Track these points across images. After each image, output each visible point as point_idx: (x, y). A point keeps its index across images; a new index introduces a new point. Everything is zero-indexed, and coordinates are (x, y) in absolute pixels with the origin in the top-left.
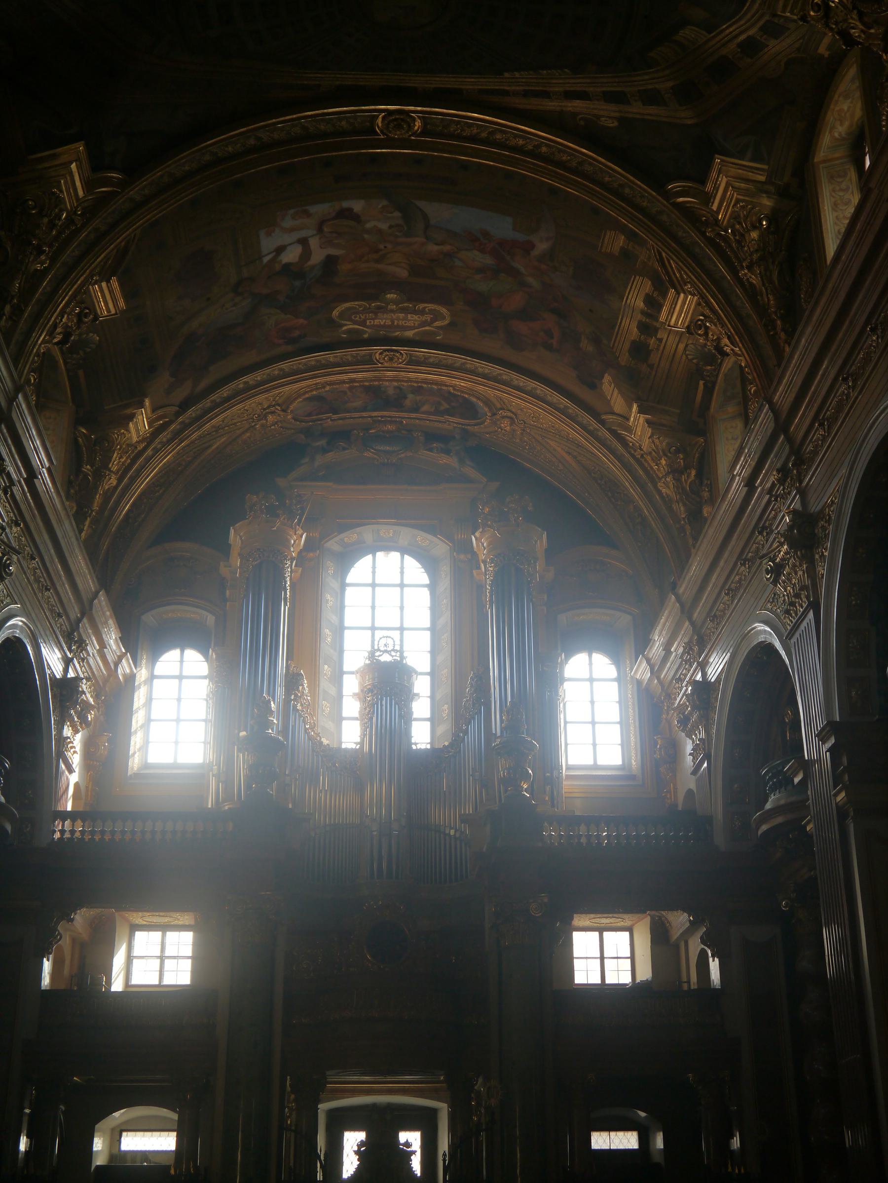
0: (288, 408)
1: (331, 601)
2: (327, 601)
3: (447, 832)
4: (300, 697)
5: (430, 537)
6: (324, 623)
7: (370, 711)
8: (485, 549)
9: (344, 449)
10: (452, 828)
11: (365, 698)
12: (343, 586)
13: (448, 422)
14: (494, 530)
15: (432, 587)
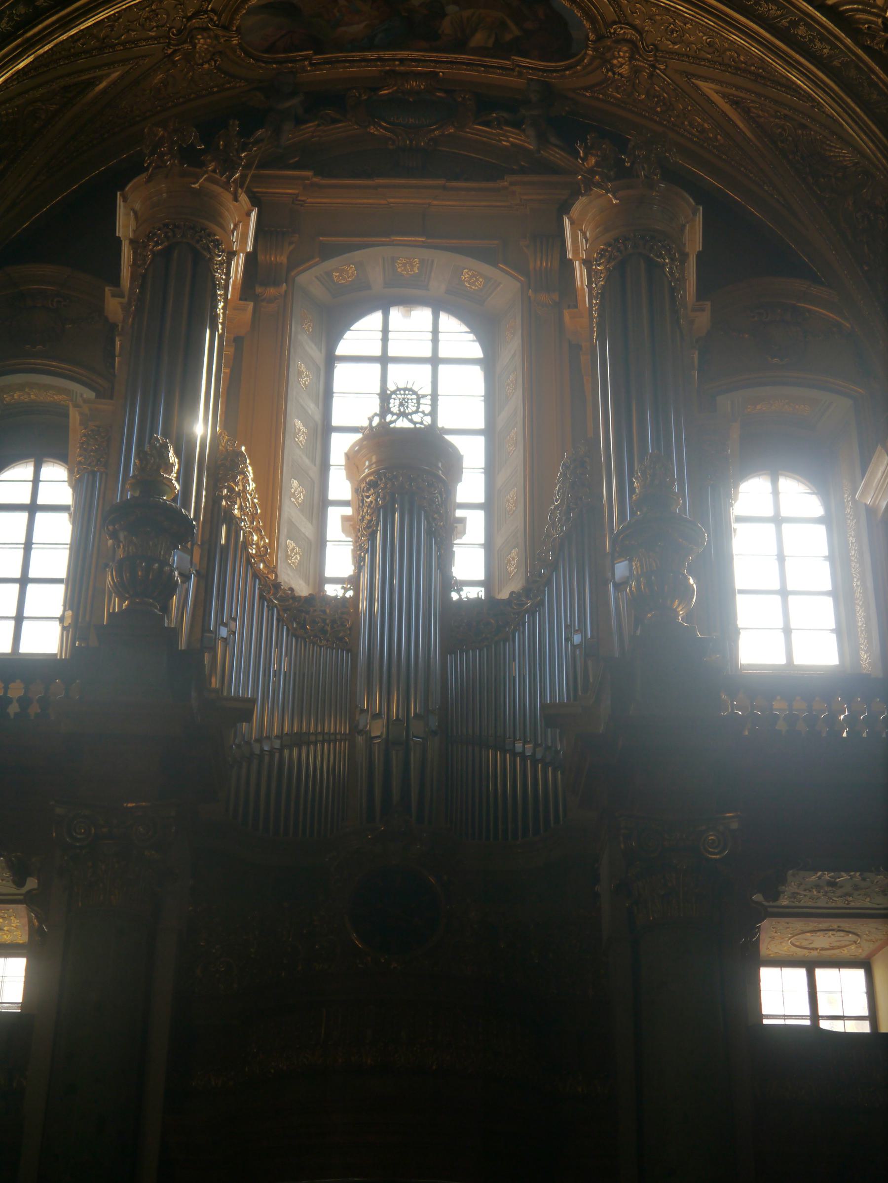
0: (232, 19)
1: (307, 376)
2: (300, 373)
3: (519, 746)
4: (238, 494)
5: (487, 269)
6: (292, 407)
7: (370, 521)
8: (587, 241)
9: (334, 121)
10: (529, 742)
11: (363, 500)
12: (331, 360)
13: (517, 69)
14: (607, 192)
15: (489, 364)
